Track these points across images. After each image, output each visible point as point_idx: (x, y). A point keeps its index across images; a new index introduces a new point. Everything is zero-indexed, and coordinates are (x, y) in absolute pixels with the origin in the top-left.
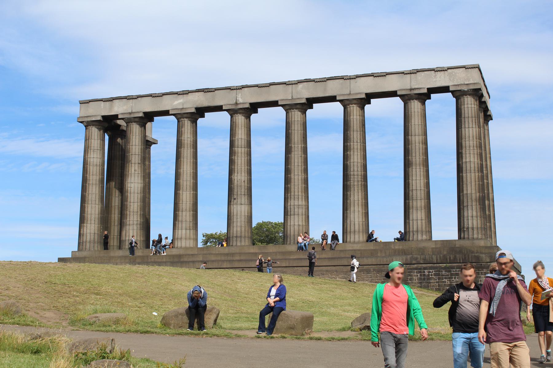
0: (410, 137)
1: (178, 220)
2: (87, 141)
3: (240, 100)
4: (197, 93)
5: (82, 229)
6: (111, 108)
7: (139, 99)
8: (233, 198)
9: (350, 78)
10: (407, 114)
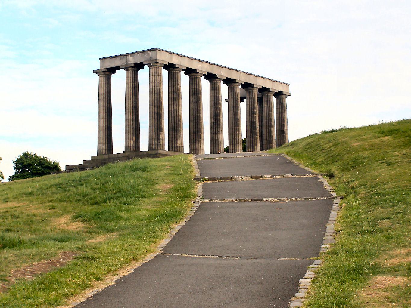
0: (272, 113)
1: (201, 138)
2: (160, 77)
3: (222, 75)
4: (206, 63)
5: (161, 136)
6: (171, 58)
7: (184, 57)
8: (221, 130)
9: (257, 76)
10: (270, 101)
